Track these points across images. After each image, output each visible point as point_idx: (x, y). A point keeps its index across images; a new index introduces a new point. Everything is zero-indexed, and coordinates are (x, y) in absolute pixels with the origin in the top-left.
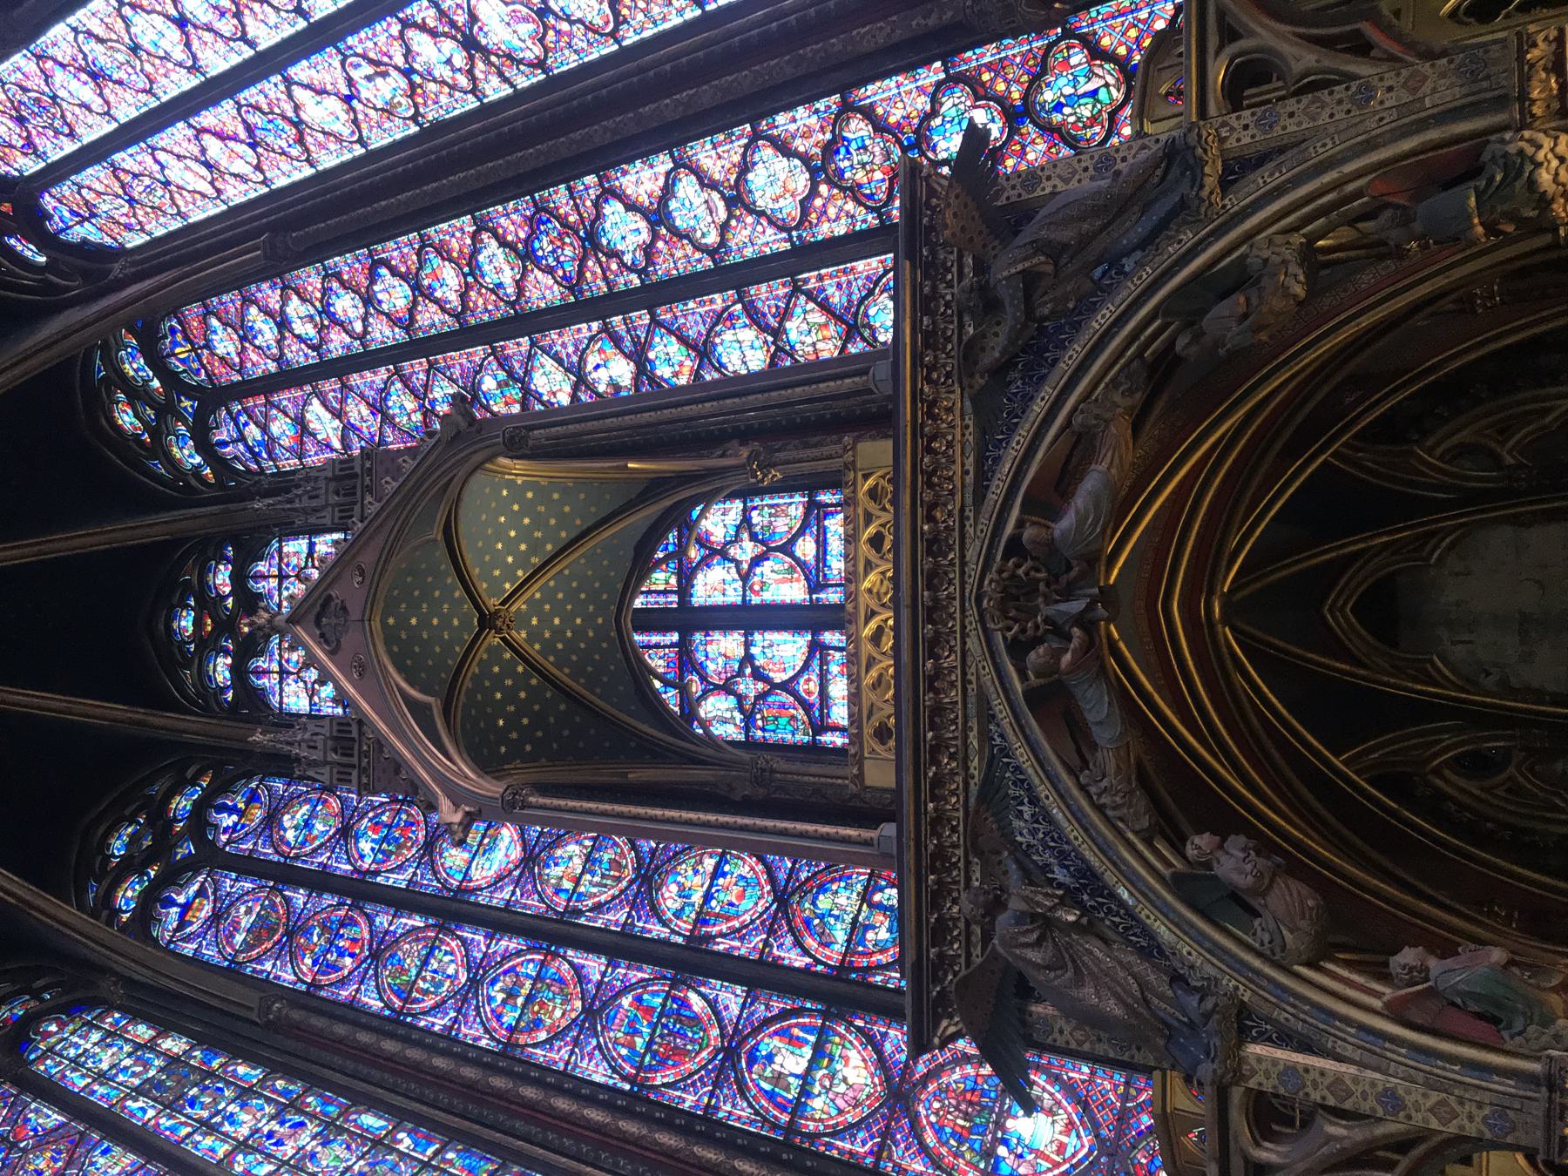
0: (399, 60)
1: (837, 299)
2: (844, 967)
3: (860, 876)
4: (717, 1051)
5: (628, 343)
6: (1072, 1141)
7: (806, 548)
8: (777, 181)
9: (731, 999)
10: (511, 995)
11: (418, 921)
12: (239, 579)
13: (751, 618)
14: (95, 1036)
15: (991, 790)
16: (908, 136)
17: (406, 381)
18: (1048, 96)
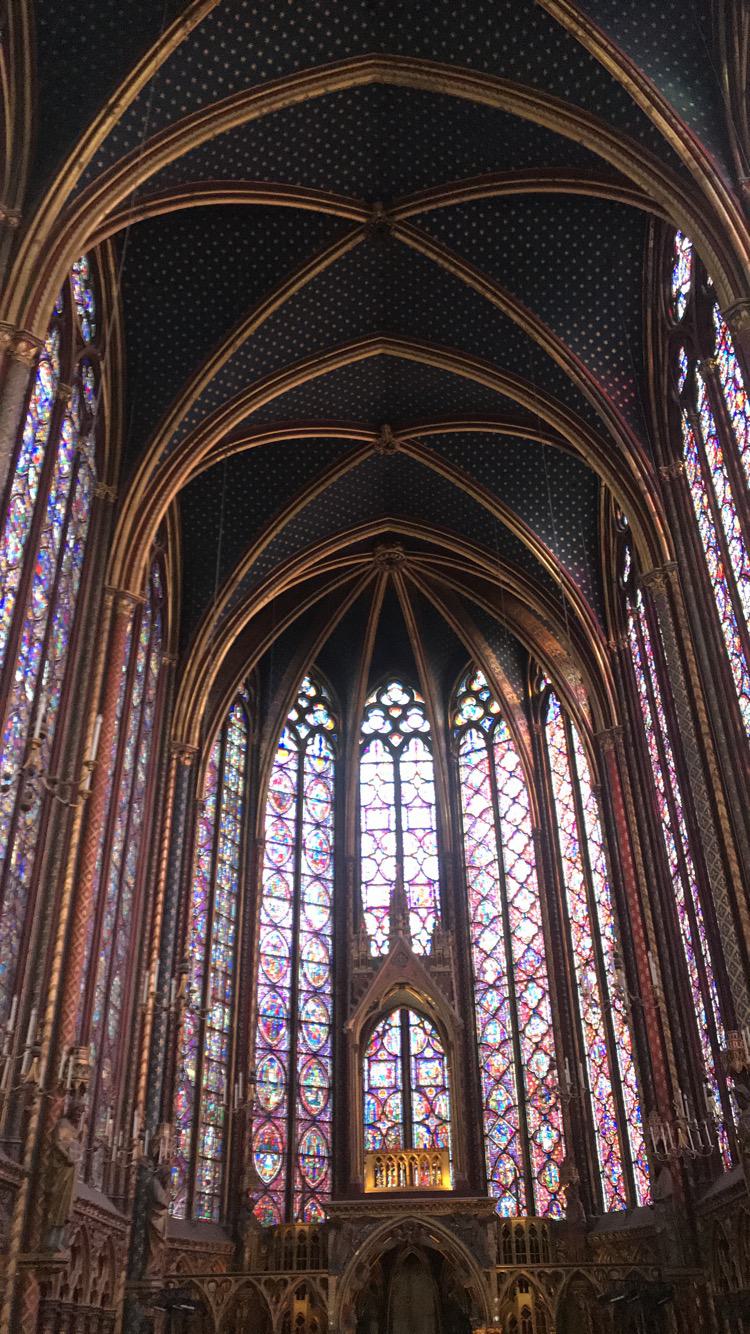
0: (587, 929)
1: (508, 1077)
2: (299, 1086)
3: (325, 1085)
4: (270, 1046)
5: (498, 983)
6: (267, 1177)
7: (429, 1053)
8: (541, 1064)
9: (285, 1046)
10: (275, 947)
11: (292, 888)
12: (416, 733)
13: (405, 1027)
14: (237, 743)
15: (374, 1220)
16: (548, 1117)
17: (491, 863)
18: (552, 1167)
